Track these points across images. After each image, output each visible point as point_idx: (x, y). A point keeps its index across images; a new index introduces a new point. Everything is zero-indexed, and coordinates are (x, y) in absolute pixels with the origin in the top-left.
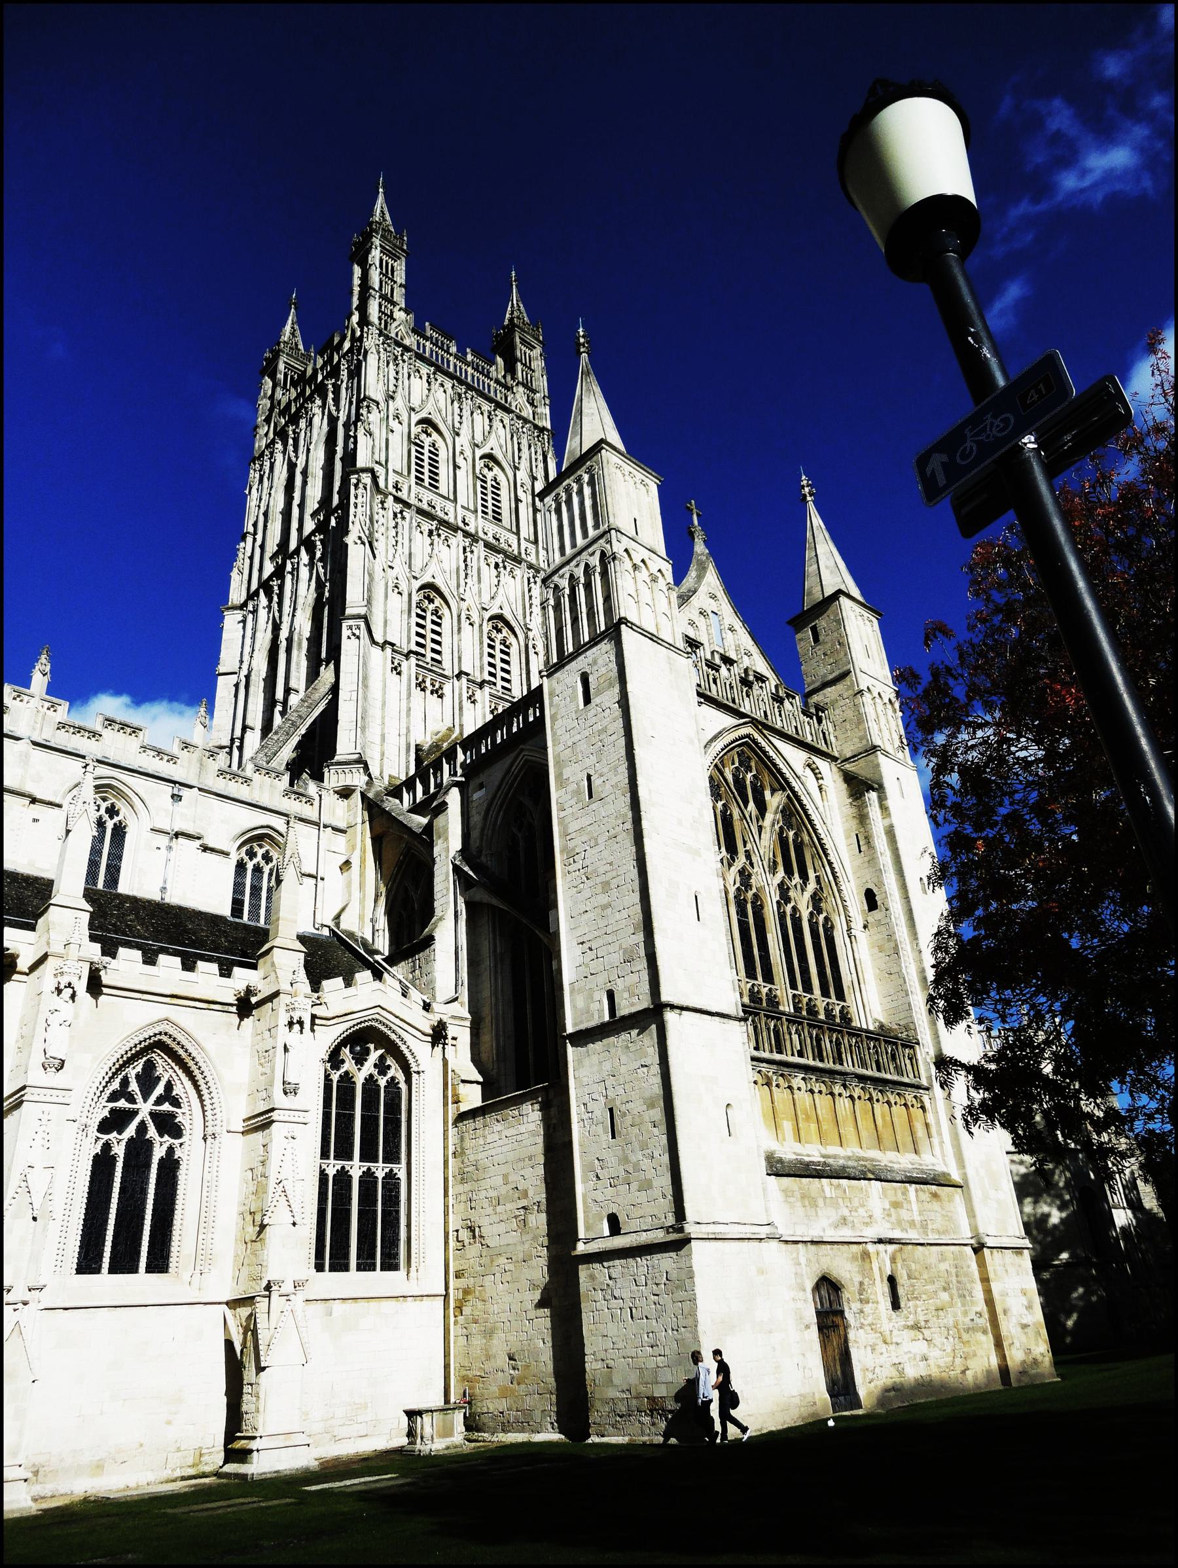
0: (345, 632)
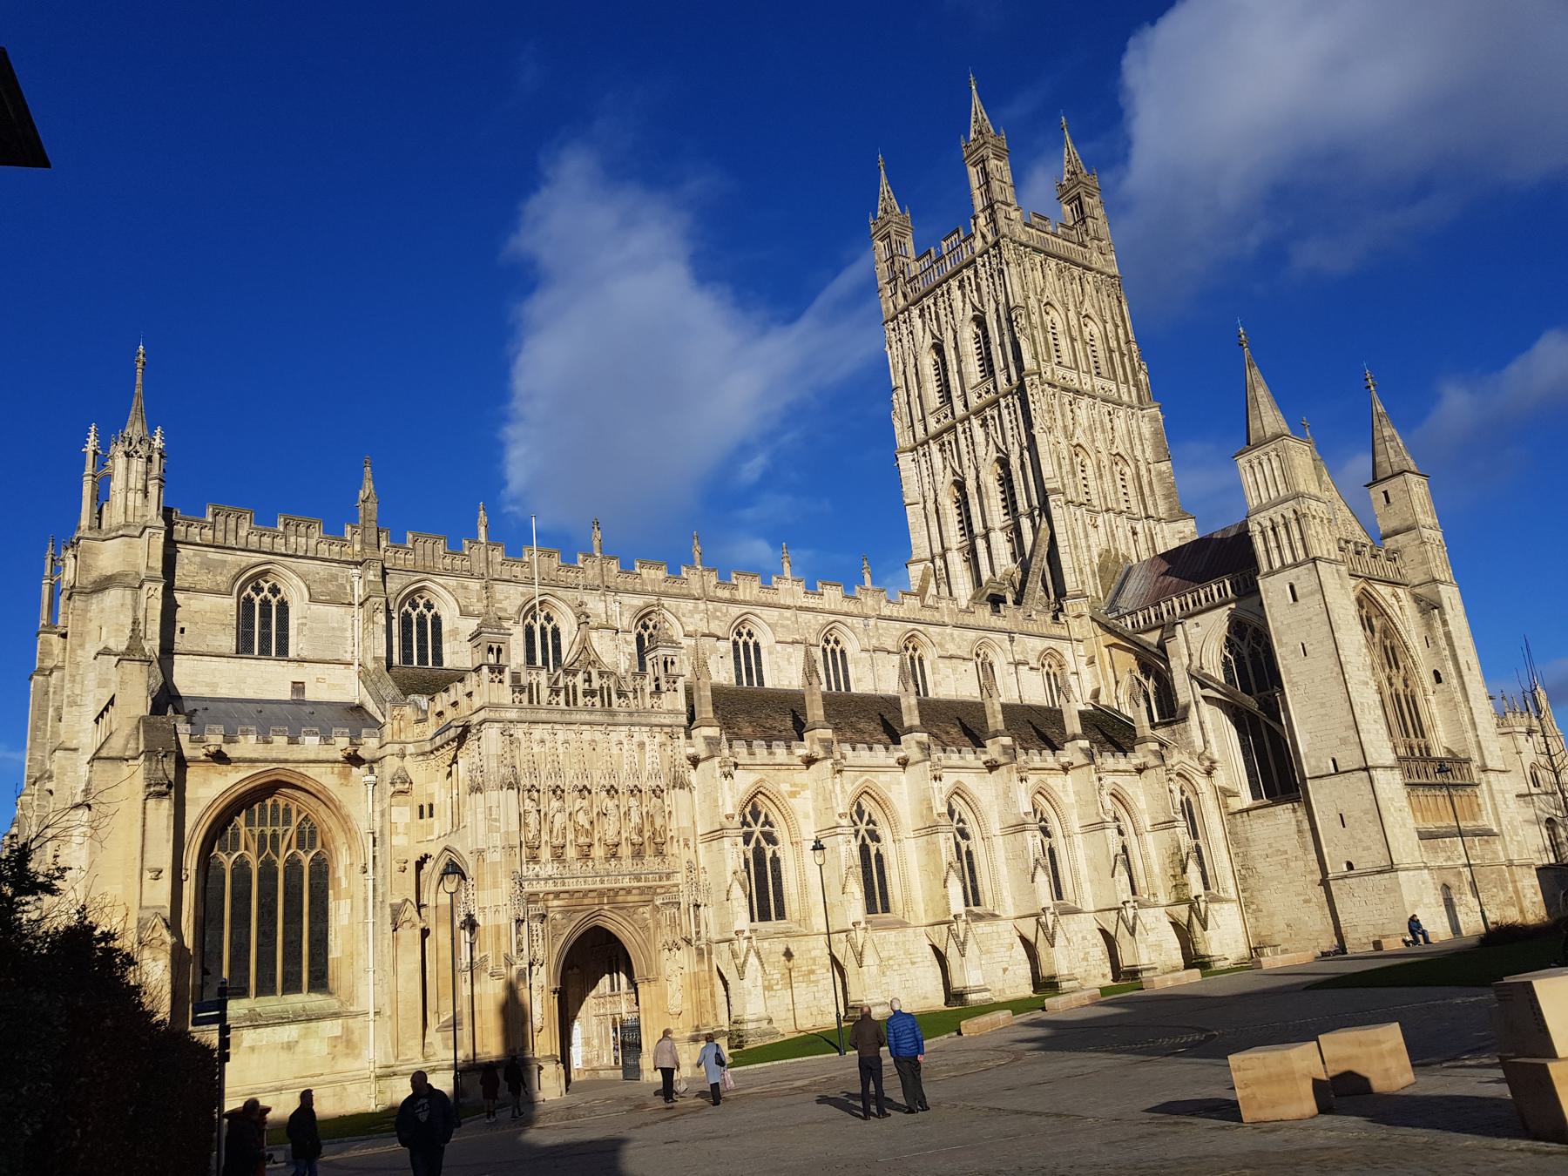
0: (1052, 504)
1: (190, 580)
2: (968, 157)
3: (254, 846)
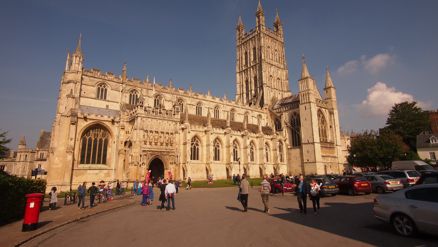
0: (264, 86)
1: (87, 83)
3: (93, 136)
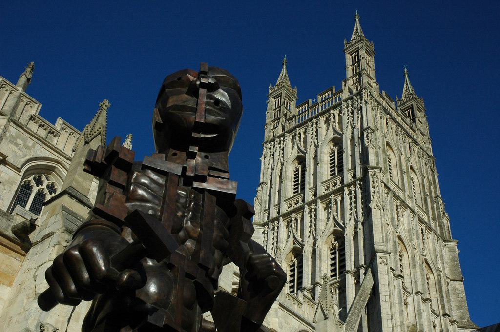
0: (379, 260)
2: (347, 48)
